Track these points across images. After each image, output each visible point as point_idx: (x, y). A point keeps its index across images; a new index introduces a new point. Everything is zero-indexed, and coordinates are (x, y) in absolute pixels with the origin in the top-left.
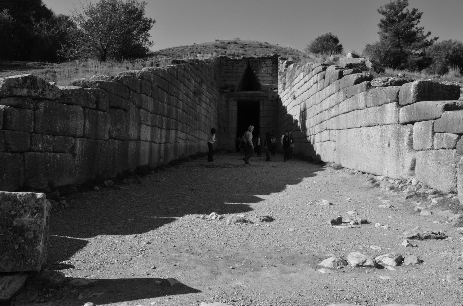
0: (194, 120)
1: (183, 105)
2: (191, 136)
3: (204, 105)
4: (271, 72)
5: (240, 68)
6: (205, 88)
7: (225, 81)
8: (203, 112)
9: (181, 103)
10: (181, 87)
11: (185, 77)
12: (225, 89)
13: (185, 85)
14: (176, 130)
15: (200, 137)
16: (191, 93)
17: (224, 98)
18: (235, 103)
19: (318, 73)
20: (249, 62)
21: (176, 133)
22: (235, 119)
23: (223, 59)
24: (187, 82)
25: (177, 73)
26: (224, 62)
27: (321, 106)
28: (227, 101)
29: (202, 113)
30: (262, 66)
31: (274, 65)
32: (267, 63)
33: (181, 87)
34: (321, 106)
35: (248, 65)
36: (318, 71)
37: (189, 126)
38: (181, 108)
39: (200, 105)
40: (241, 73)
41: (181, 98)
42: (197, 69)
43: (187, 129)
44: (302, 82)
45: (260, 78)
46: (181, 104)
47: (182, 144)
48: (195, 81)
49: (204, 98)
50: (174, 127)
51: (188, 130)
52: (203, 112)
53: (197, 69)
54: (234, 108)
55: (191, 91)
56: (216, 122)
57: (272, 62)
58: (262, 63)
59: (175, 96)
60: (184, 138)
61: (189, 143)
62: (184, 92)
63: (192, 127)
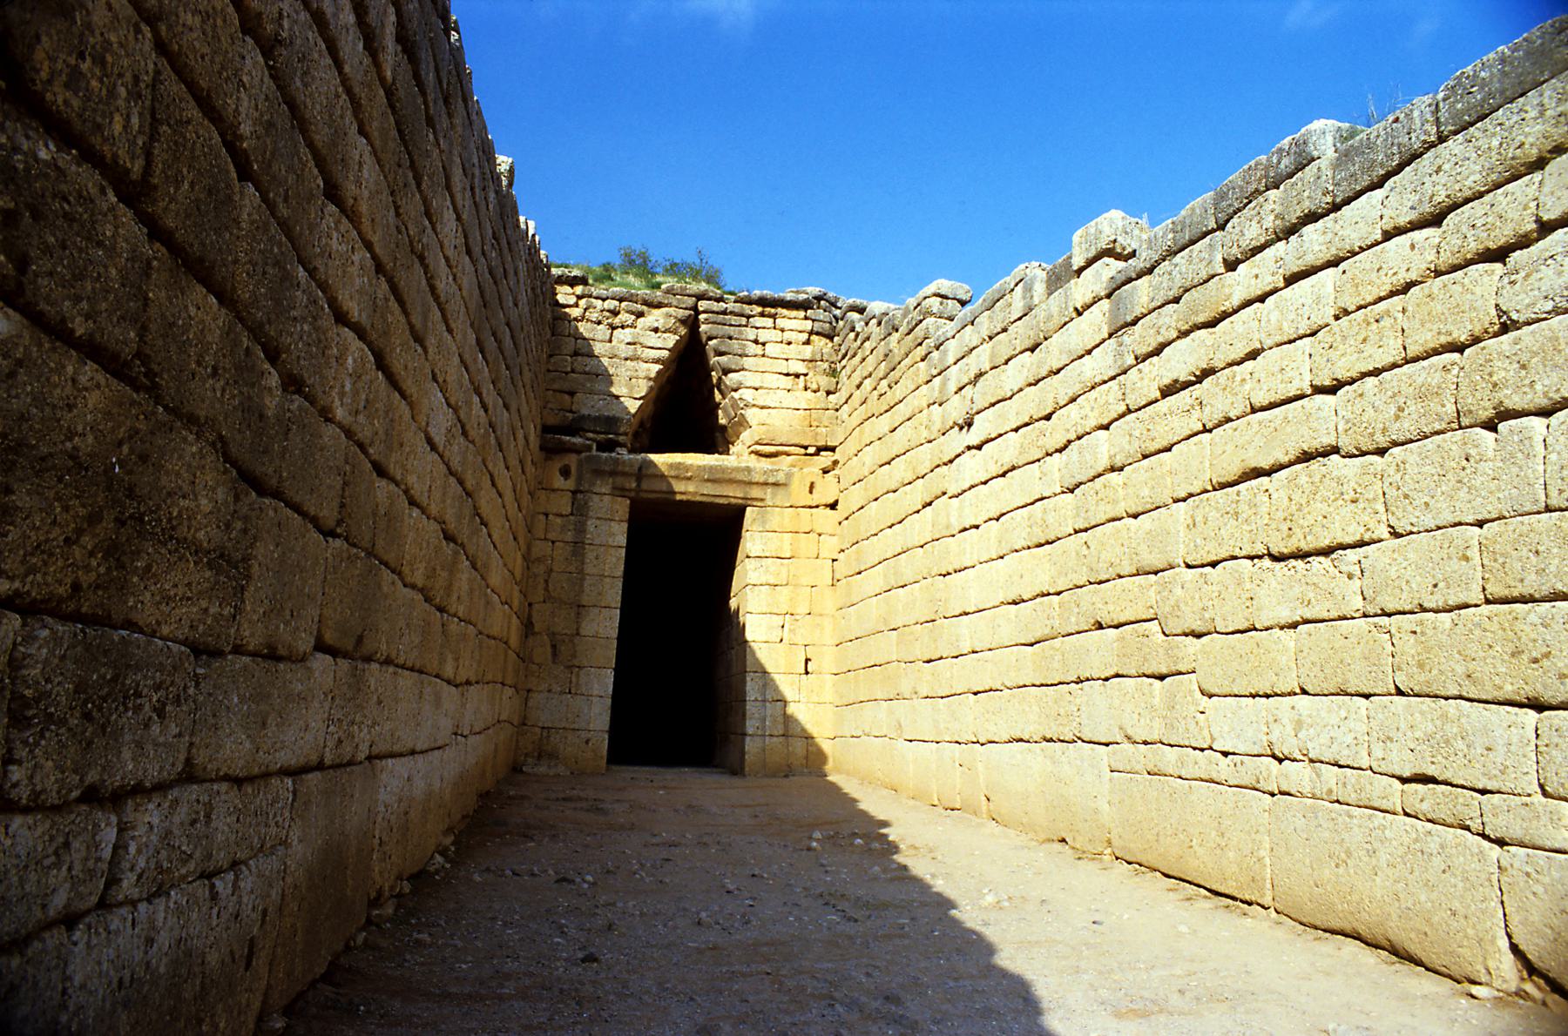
4: (800, 368)
5: (653, 339)
7: (572, 394)
18: (622, 507)
20: (697, 313)
22: (614, 594)
23: (567, 289)
26: (572, 300)
28: (574, 493)
30: (763, 336)
31: (814, 337)
32: (780, 322)
35: (692, 323)
40: (656, 361)
54: (611, 535)
56: (516, 603)
57: (808, 325)
58: (759, 321)
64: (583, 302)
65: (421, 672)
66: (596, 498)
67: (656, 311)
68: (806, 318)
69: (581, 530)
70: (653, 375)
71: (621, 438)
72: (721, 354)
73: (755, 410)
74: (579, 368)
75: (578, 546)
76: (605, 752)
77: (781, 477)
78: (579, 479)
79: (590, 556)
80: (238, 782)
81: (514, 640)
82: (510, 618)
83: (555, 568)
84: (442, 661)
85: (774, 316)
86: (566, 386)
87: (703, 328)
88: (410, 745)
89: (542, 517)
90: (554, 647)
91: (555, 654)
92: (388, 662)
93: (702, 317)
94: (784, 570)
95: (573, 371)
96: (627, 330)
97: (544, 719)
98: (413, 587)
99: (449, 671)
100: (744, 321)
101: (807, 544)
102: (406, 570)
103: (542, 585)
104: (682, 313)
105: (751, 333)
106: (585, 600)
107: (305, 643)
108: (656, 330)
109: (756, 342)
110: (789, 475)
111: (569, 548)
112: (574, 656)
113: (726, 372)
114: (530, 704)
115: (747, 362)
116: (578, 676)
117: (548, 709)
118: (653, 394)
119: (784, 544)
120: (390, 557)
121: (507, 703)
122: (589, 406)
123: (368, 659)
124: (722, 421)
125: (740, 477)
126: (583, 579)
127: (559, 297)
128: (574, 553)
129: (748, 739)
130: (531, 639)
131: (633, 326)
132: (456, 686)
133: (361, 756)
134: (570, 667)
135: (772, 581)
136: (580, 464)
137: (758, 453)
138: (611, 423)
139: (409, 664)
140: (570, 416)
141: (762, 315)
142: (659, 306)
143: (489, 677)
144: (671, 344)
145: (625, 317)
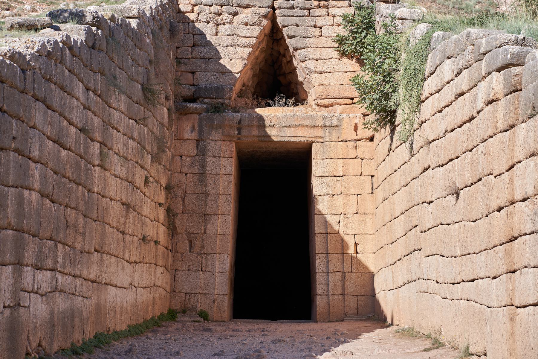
0: (81, 219)
1: (43, 176)
2: (70, 279)
3: (116, 165)
5: (244, 31)
6: (122, 107)
7: (193, 73)
8: (116, 189)
9: (36, 170)
10: (38, 114)
11: (49, 80)
12: (193, 99)
13: (48, 107)
14: (19, 264)
15: (104, 278)
16: (73, 130)
17: (188, 134)
19: (499, 70)
20: (274, 9)
21: (18, 275)
24: (57, 97)
25: (23, 71)
27: (511, 181)
29: (112, 194)
32: (332, 11)
33: (38, 114)
34: (511, 181)
36: (499, 65)
37: (65, 244)
38: (37, 186)
39: (102, 167)
41: (35, 153)
42: (93, 47)
43: (56, 257)
44: (448, 93)
45: (311, 65)
46: (37, 177)
47: (38, 308)
48: (88, 89)
49: (118, 141)
50: (8, 258)
51: (60, 260)
52: (116, 189)
53: (93, 47)
55: (71, 124)
58: (317, 12)
59: (16, 151)
60: (45, 287)
61: (61, 303)
62: (48, 130)
63: (73, 247)
64: (196, 9)
65: (117, 257)
66: (212, 144)
67: (246, 11)
68: (350, 6)
69: (203, 165)
70: (246, 56)
71: (227, 102)
72: (292, 37)
73: (316, 75)
74: (196, 54)
75: (202, 176)
76: (226, 308)
77: (334, 122)
78: (201, 132)
79: (210, 181)
80: (85, 280)
81: (162, 238)
82: (158, 227)
83: (188, 191)
84: (124, 253)
85: (327, 7)
86: (189, 68)
87: (279, 20)
88: (115, 283)
89: (178, 158)
90: (190, 242)
91: (191, 247)
92: (108, 253)
93: (277, 12)
94: (339, 185)
95: (192, 58)
96: (227, 26)
97: (186, 288)
98: (113, 227)
99: (127, 257)
100: (306, 12)
101: (354, 166)
102: (111, 222)
103: (180, 203)
104: (264, 11)
105: (310, 21)
106: (209, 210)
107: (93, 250)
108: (246, 24)
109: (315, 26)
110: (340, 120)
111: (197, 178)
112: (203, 247)
113: (296, 49)
114: (177, 279)
115: (310, 42)
116: (206, 259)
117: (189, 282)
118: (249, 66)
119: (339, 167)
120: (107, 221)
121: (160, 277)
122: (205, 79)
123: (104, 253)
124: (300, 79)
125: (307, 123)
126: (206, 197)
127: (180, 6)
128: (200, 181)
129: (318, 298)
130: (175, 237)
131: (231, 22)
132: (130, 263)
133: (103, 282)
134: (201, 254)
135: (331, 192)
136: (200, 120)
137: (318, 105)
138: (219, 90)
139: (114, 254)
140: (193, 89)
141: (319, 7)
142: (247, 7)
143: (147, 260)
144: (257, 33)
145: (226, 17)
